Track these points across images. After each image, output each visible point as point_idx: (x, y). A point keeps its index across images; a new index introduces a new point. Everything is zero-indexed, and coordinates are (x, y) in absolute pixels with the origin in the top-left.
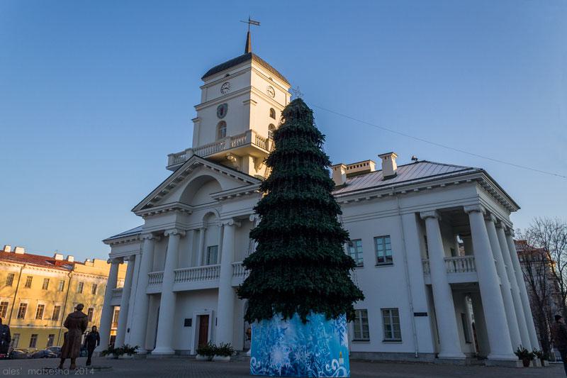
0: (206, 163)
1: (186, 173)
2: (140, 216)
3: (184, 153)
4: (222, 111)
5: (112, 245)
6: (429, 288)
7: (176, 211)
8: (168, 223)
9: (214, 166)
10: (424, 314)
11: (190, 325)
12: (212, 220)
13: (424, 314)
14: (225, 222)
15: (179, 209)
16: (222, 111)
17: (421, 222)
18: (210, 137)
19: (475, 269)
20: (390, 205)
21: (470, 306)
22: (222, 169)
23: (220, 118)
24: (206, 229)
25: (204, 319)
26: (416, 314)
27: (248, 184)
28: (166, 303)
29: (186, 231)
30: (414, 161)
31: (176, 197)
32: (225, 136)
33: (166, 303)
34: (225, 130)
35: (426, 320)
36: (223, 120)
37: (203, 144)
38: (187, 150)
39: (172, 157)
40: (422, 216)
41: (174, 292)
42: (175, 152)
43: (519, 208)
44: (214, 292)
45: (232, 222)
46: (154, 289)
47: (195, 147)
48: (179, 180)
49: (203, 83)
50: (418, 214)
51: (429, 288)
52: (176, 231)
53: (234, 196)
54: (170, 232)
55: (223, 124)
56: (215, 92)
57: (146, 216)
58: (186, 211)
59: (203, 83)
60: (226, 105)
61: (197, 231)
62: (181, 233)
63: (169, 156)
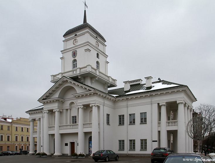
0: (69, 81)
1: (60, 85)
2: (42, 103)
3: (58, 75)
4: (74, 54)
5: (30, 114)
6: (159, 132)
7: (57, 101)
8: (54, 106)
9: (73, 82)
10: (157, 141)
11: (67, 146)
12: (73, 105)
13: (157, 141)
14: (79, 107)
15: (59, 101)
16: (74, 54)
17: (159, 107)
18: (69, 67)
19: (177, 125)
20: (148, 100)
21: (172, 137)
22: (77, 83)
23: (73, 58)
24: (71, 109)
25: (73, 144)
26: (153, 141)
27: (89, 91)
28: (57, 138)
29: (62, 110)
30: (159, 80)
31: (56, 95)
32: (76, 67)
33: (57, 138)
34: (76, 64)
35: (157, 143)
36: (75, 58)
37: (66, 71)
38: (59, 74)
39: (53, 77)
40: (160, 104)
41: (60, 134)
42: (54, 74)
43: (197, 100)
44: (76, 134)
45: (82, 107)
46: (52, 132)
47: (63, 72)
48: (57, 88)
49: (64, 39)
50: (158, 104)
51: (159, 132)
52: (58, 110)
53: (83, 96)
54: (56, 110)
55: (75, 61)
56: (70, 44)
57: (44, 103)
58: (62, 101)
59: (64, 39)
60: (76, 51)
61: (67, 110)
62: (60, 110)
63: (51, 76)
